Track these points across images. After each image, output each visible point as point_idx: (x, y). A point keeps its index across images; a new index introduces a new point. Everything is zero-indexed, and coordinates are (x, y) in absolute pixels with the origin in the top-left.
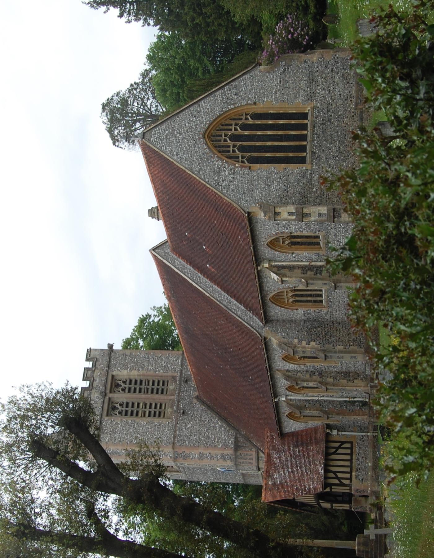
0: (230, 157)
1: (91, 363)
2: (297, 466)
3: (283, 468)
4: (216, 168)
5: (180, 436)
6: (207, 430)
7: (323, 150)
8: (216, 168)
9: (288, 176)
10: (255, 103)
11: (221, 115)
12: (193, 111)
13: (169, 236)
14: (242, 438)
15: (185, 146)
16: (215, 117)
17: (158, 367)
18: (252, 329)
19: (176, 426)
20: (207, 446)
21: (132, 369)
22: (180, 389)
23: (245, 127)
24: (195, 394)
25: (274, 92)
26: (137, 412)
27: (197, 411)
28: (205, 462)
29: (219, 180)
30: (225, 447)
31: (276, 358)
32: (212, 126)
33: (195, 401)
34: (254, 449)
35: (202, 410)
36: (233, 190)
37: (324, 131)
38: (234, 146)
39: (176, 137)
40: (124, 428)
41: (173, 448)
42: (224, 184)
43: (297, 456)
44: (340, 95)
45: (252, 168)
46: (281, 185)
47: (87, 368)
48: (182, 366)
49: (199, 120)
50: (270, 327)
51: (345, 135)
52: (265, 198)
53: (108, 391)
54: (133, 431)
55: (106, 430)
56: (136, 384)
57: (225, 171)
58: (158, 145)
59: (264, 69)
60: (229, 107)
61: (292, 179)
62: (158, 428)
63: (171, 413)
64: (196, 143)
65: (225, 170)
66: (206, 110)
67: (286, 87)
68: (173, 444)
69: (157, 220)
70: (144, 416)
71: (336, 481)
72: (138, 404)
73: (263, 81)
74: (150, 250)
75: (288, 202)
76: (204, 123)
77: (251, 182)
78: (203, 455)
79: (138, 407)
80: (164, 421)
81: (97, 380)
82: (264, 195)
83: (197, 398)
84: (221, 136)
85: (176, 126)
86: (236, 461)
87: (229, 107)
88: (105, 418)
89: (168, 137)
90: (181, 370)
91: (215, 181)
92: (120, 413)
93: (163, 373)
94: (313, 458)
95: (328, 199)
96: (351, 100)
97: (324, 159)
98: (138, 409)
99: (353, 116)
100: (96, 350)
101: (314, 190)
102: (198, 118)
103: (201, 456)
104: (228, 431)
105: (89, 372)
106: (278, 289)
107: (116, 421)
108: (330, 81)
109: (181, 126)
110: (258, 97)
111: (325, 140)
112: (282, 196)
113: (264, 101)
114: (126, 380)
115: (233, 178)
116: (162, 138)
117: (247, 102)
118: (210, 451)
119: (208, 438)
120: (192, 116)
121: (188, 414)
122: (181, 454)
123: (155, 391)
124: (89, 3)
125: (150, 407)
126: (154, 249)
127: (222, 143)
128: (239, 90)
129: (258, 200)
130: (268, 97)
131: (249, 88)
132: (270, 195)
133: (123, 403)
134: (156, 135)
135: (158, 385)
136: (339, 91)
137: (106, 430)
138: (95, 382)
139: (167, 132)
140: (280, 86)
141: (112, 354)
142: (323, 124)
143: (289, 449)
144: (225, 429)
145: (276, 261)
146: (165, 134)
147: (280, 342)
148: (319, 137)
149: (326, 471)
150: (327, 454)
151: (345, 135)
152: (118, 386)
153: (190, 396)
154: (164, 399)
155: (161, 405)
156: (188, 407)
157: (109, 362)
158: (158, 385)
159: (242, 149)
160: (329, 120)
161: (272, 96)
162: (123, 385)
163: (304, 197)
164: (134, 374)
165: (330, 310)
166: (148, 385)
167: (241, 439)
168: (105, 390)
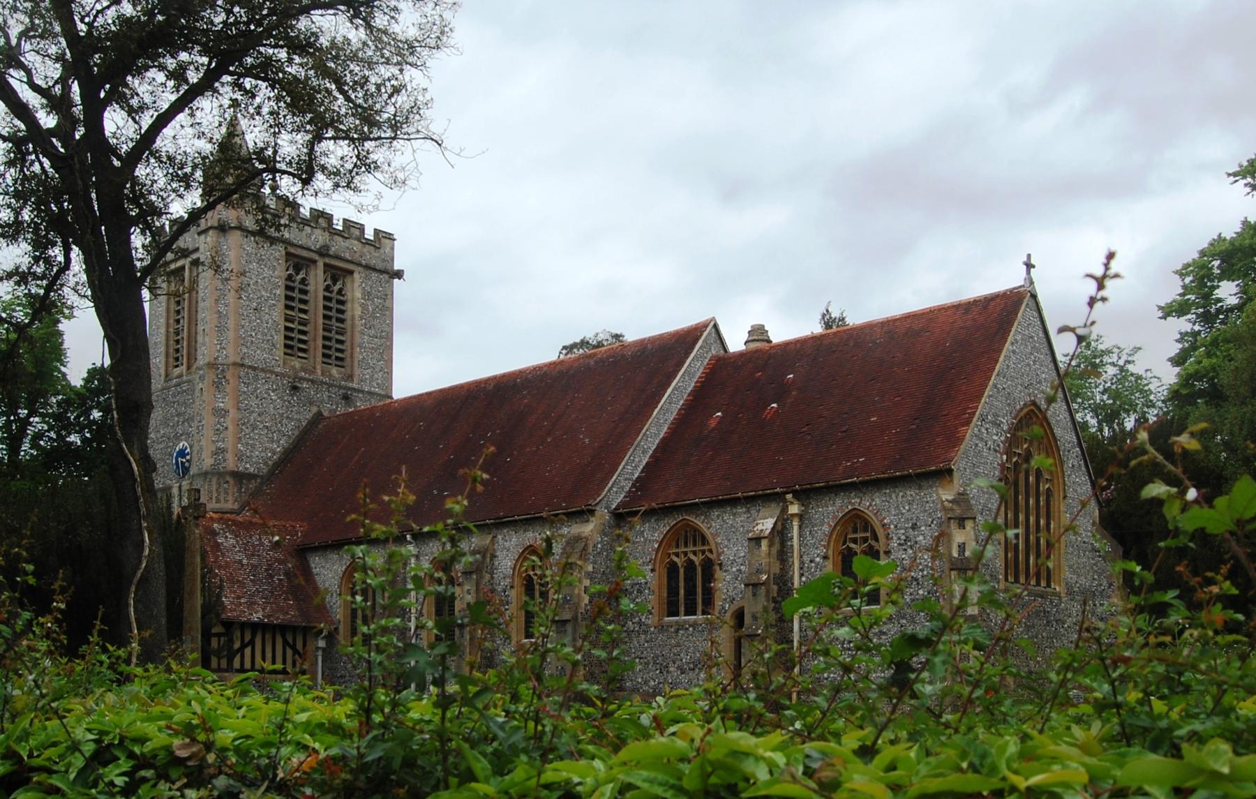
1: (372, 238)
2: (254, 575)
3: (245, 550)
5: (256, 379)
6: (267, 427)
13: (786, 345)
14: (256, 487)
18: (607, 489)
19: (272, 372)
20: (240, 424)
21: (364, 307)
22: (332, 385)
27: (297, 413)
28: (209, 420)
30: (240, 457)
31: (530, 534)
33: (315, 409)
34: (236, 506)
35: (299, 420)
41: (235, 364)
43: (271, 577)
47: (364, 230)
50: (609, 522)
63: (293, 367)
68: (242, 365)
69: (745, 339)
71: (237, 645)
72: (305, 312)
74: (713, 319)
78: (224, 417)
80: (280, 352)
81: (347, 243)
83: (319, 414)
86: (213, 474)
94: (274, 603)
98: (297, 310)
100: (392, 249)
103: (221, 413)
104: (266, 464)
105: (357, 232)
106: (716, 535)
114: (343, 296)
118: (231, 428)
119: (254, 427)
121: (292, 395)
122: (224, 377)
123: (327, 343)
124: (827, 311)
126: (716, 326)
141: (387, 276)
143: (280, 562)
144: (270, 458)
145: (800, 527)
147: (587, 538)
149: (255, 627)
150: (283, 629)
154: (315, 357)
157: (374, 270)
162: (336, 288)
164: (355, 310)
165: (652, 629)
167: (253, 485)
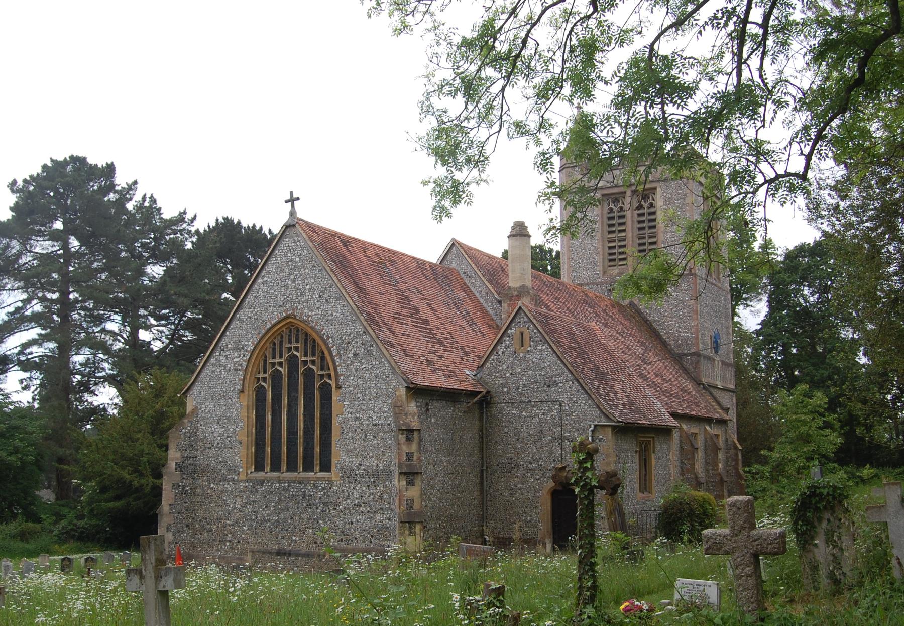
10: (339, 387)
11: (321, 337)
12: (330, 292)
16: (318, 327)
19: (593, 284)
23: (309, 374)
25: (358, 416)
26: (614, 232)
36: (213, 372)
38: (280, 364)
39: (290, 275)
44: (352, 523)
45: (242, 395)
49: (315, 304)
51: (287, 530)
56: (650, 220)
57: (239, 357)
59: (400, 396)
60: (335, 347)
61: (227, 453)
63: (611, 275)
64: (280, 306)
66: (330, 312)
67: (366, 435)
70: (610, 242)
72: (624, 231)
73: (378, 397)
76: (310, 313)
77: (225, 396)
79: (620, 231)
85: (307, 271)
87: (335, 347)
89: (290, 263)
91: (227, 345)
92: (611, 210)
96: (341, 540)
97: (252, 498)
99: (316, 543)
101: (212, 485)
108: (376, 506)
109: (306, 279)
110: (351, 391)
111: (280, 499)
113: (344, 401)
116: (289, 255)
117: (342, 375)
129: (201, 409)
130: (350, 406)
131: (367, 375)
136: (357, 521)
139: (297, 259)
140: (368, 425)
142: (305, 495)
146: (294, 257)
148: (284, 490)
151: (287, 530)
152: (645, 197)
159: (276, 377)
160: (309, 506)
161: (351, 413)
163: (203, 471)
164: (660, 216)
166: (650, 237)
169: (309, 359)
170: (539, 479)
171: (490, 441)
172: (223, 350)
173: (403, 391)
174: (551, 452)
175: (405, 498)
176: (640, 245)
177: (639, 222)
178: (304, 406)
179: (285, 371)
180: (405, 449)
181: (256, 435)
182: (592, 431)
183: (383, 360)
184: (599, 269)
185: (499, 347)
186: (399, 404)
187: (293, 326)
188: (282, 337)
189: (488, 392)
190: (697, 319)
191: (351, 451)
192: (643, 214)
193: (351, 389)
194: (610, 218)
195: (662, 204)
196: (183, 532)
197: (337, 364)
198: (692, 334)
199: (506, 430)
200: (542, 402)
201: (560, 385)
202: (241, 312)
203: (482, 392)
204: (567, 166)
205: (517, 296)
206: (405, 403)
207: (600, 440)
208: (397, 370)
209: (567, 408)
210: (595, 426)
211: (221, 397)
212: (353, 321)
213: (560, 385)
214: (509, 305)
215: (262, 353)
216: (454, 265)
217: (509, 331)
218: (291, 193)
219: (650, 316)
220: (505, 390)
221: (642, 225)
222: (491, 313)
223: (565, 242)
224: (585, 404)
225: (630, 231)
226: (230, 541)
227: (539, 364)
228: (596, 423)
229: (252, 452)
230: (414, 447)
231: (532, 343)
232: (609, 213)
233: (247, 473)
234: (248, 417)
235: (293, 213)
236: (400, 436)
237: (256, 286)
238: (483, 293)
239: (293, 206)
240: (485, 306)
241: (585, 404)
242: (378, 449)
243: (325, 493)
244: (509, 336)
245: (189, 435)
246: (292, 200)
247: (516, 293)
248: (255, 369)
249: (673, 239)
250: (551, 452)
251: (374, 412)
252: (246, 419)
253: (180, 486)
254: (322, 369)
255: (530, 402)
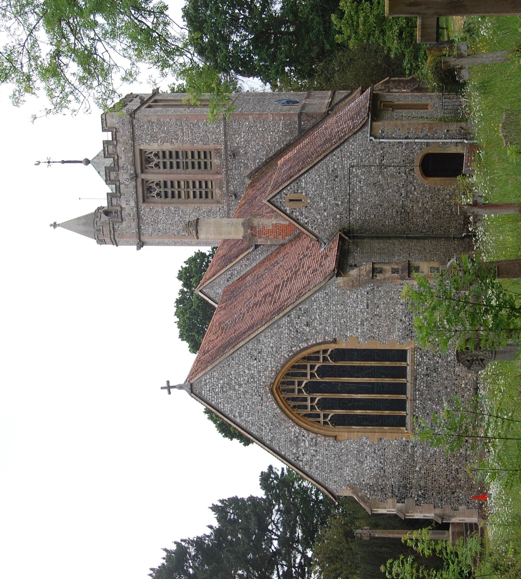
0: (309, 416)
1: (110, 133)
4: (292, 437)
7: (428, 414)
8: (292, 437)
9: (385, 449)
10: (335, 341)
11: (291, 358)
12: (252, 349)
15: (248, 404)
17: (195, 136)
21: (163, 141)
22: (227, 167)
23: (323, 371)
24: (246, 172)
25: (359, 323)
26: (179, 193)
29: (299, 454)
32: (280, 375)
36: (317, 468)
37: (428, 386)
38: (312, 400)
39: (235, 390)
40: (167, 217)
42: (305, 459)
45: (338, 438)
46: (376, 461)
48: (225, 135)
49: (262, 365)
52: (358, 478)
53: (139, 171)
54: (179, 220)
55: (146, 220)
56: (171, 157)
58: (212, 401)
59: (344, 282)
60: (300, 345)
61: (389, 453)
62: (207, 215)
63: (221, 196)
65: (304, 440)
66: (270, 349)
70: (189, 197)
72: (179, 183)
73: (344, 303)
75: (386, 484)
76: (270, 369)
79: (179, 186)
82: (356, 475)
84: (293, 383)
85: (232, 372)
87: (300, 345)
88: (143, 206)
89: (224, 390)
90: (226, 142)
91: (294, 454)
92: (158, 195)
93: (203, 146)
95: (435, 481)
101: (417, 469)
102: (260, 361)
105: (111, 147)
107: (156, 209)
109: (239, 373)
110: (338, 329)
111: (430, 400)
112: (379, 477)
113: (346, 336)
114: (158, 152)
115: (316, 451)
116: (217, 390)
117: (324, 338)
120: (251, 357)
123: (196, 166)
125: (194, 186)
127: (296, 394)
128: (311, 318)
129: (349, 481)
130: (351, 330)
131: (325, 314)
132: (362, 475)
133: (160, 182)
134: (208, 387)
135: (199, 157)
137: (146, 220)
138: (120, 160)
139: (221, 382)
140: (368, 313)
141: (134, 121)
142: (427, 375)
148: (422, 395)
152: (148, 160)
153: (241, 175)
155: (206, 183)
156: (240, 189)
157: (133, 133)
158: (199, 157)
159: (324, 404)
160: (435, 370)
161: (357, 329)
162: (156, 160)
163: (405, 478)
164: (167, 147)
166: (187, 158)
168: (135, 171)
169: (309, 371)
170: (415, 187)
171: (382, 231)
172: (298, 457)
173: (340, 280)
174: (392, 176)
175: (430, 273)
176: (193, 167)
177: (171, 167)
178: (349, 377)
179: (319, 396)
180: (388, 274)
181: (374, 426)
182: (375, 138)
183: (313, 298)
184: (215, 207)
185: (302, 222)
186: (351, 283)
187: (279, 387)
188: (288, 399)
189: (339, 231)
190: (267, 114)
191: (389, 330)
192: (164, 163)
193: (336, 329)
194: (166, 196)
195: (156, 144)
196: (459, 497)
197: (314, 342)
198: (281, 120)
199: (372, 216)
200: (349, 183)
201: (335, 167)
202: (265, 439)
203: (340, 235)
204: (112, 236)
205: (251, 230)
206: (350, 278)
207: (383, 132)
208: (322, 284)
209: (355, 161)
210: (371, 136)
211: (340, 459)
212: (279, 327)
213: (335, 167)
214: (260, 238)
215: (302, 419)
216: (220, 291)
217: (288, 212)
218: (162, 388)
219: (262, 159)
220: (338, 216)
221: (175, 165)
222: (265, 255)
223: (187, 241)
224: (353, 145)
225: (180, 176)
226: (466, 450)
227: (317, 185)
228: (368, 135)
229: (389, 429)
230: (387, 267)
231: (299, 191)
232: (161, 197)
233: (407, 433)
234: (358, 432)
235: (180, 387)
236: (378, 278)
237: (243, 424)
238: (247, 263)
239: (174, 387)
240: (259, 261)
241: (353, 145)
242: (388, 303)
243: (425, 355)
244: (293, 212)
245: (372, 492)
246: (169, 388)
247: (249, 231)
248: (316, 426)
249: (190, 135)
250: (392, 176)
251: (357, 307)
252: (360, 434)
253: (418, 500)
254: (318, 359)
255: (349, 194)
